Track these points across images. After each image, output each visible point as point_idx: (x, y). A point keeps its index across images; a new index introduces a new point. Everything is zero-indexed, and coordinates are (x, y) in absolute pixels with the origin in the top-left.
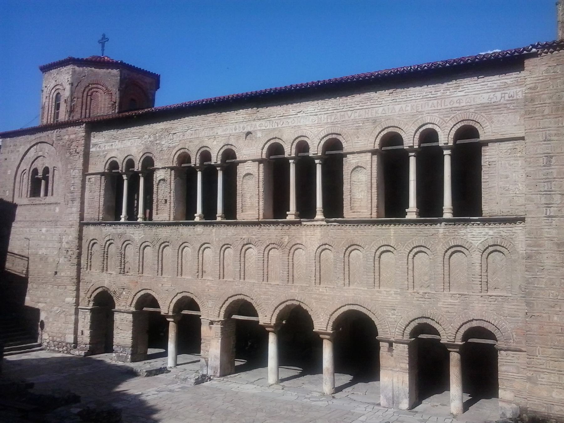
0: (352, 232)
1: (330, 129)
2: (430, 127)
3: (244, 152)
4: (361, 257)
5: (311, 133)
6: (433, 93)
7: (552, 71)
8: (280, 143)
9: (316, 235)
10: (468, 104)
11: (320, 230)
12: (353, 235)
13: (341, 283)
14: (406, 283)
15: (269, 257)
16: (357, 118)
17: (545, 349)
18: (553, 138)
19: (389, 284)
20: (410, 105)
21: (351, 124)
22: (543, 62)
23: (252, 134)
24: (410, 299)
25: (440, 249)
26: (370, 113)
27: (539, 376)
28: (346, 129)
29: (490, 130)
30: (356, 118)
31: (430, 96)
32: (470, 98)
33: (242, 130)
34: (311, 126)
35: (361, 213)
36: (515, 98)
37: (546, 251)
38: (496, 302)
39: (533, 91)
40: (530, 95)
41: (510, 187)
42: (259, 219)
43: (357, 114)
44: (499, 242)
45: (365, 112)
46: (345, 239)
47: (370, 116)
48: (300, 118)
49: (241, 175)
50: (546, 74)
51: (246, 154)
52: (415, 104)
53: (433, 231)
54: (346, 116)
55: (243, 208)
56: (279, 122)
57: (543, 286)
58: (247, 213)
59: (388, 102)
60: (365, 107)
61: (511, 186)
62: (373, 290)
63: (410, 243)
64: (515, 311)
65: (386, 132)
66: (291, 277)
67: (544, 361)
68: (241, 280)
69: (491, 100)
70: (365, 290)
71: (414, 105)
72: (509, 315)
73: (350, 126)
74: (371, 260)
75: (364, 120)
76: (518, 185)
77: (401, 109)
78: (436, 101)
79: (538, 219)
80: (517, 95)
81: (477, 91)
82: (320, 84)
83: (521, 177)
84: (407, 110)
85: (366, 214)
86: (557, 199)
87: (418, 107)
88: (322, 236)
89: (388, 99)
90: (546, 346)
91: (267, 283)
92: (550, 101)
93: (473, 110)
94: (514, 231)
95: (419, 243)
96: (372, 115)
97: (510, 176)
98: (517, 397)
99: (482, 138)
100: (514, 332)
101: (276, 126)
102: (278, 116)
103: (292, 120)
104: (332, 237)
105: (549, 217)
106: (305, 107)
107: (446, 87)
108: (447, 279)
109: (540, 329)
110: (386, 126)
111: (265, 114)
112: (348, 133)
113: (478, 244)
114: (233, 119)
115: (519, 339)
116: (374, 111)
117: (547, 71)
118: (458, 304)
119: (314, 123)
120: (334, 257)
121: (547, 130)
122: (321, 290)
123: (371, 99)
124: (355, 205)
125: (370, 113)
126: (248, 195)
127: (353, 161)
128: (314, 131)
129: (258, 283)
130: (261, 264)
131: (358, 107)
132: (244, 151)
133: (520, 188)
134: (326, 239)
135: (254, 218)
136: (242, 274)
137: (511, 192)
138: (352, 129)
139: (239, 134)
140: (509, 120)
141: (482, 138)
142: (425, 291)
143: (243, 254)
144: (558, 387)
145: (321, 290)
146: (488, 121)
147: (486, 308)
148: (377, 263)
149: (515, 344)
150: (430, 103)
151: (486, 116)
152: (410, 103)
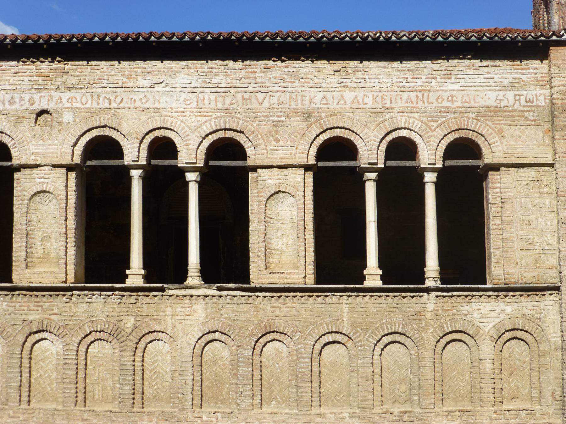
0: (268, 308)
1: (222, 121)
2: (405, 135)
3: (32, 148)
4: (285, 355)
5: (183, 125)
6: (409, 80)
8: (114, 137)
9: (196, 314)
10: (466, 104)
11: (204, 306)
12: (270, 314)
13: (245, 403)
14: (371, 397)
15: (89, 358)
16: (276, 106)
19: (337, 400)
20: (370, 95)
21: (263, 116)
23: (51, 114)
26: (299, 101)
28: (255, 125)
29: (500, 148)
30: (273, 106)
31: (404, 84)
32: (468, 95)
33: (27, 105)
34: (182, 112)
35: (285, 276)
36: (535, 104)
38: (518, 420)
40: (560, 102)
41: (535, 240)
42: (66, 282)
43: (275, 100)
44: (521, 324)
45: (290, 98)
46: (255, 322)
47: (300, 106)
48: (159, 94)
49: (26, 193)
51: (37, 153)
52: (380, 94)
53: (417, 307)
54: (253, 100)
55: (29, 260)
56: (113, 99)
58: (36, 270)
59: (332, 85)
60: (289, 89)
61: (536, 237)
62: (309, 412)
63: (377, 328)
65: (328, 136)
66: (138, 397)
68: (22, 406)
69: (500, 103)
70: (295, 414)
71: (377, 96)
73: (261, 118)
74: (306, 360)
75: (288, 111)
76: (547, 237)
77: (355, 100)
78: (413, 95)
80: (537, 99)
81: (479, 86)
82: (222, 38)
83: (549, 224)
84: (367, 103)
85: (295, 276)
87: (385, 99)
88: (207, 316)
89: (333, 80)
91: (83, 409)
93: (473, 115)
94: (542, 307)
95: (393, 328)
96: (302, 104)
97: (534, 222)
99: (488, 159)
101: (107, 105)
102: (110, 86)
103: (141, 95)
104: (229, 318)
106: (171, 76)
107: (430, 72)
108: (438, 388)
110: (328, 126)
111: (82, 80)
112: (258, 131)
113: (489, 328)
114: (7, 83)
116: (307, 98)
119: (189, 106)
120: (231, 354)
122: (205, 418)
123: (298, 76)
124: (271, 260)
125: (299, 101)
126: (38, 235)
127: (270, 181)
128: (190, 121)
129: (64, 410)
130: (71, 372)
131: (277, 88)
132: (31, 147)
133: (550, 241)
134: (217, 322)
135: (56, 280)
136: (25, 394)
137: (537, 247)
138: (265, 125)
139: (19, 112)
140: (528, 136)
141: (488, 159)
142: (403, 409)
143: (28, 352)
145: (205, 418)
148: (316, 364)
150: (405, 95)
151: (493, 126)
152: (371, 91)
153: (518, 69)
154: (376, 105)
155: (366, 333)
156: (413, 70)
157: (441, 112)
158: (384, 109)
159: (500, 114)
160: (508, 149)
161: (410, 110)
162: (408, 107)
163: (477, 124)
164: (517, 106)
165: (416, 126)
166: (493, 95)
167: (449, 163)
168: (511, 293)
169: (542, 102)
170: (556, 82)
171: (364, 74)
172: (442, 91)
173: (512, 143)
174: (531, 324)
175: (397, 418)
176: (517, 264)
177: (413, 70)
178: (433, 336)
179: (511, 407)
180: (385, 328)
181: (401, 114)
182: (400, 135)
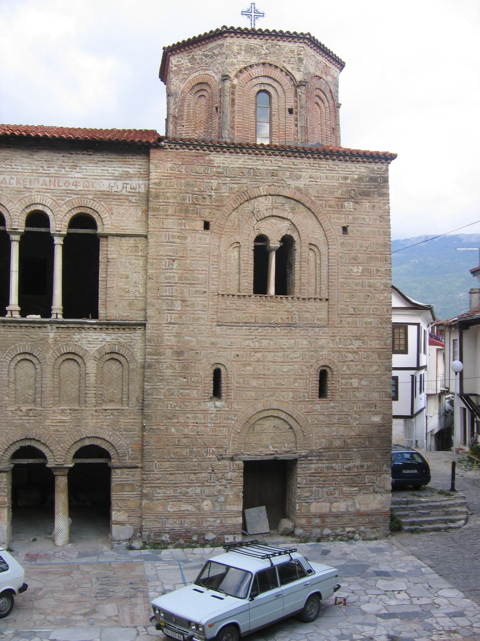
2: (40, 209)
6: (45, 168)
7: (177, 170)
10: (86, 189)
17: (161, 463)
18: (176, 240)
20: (15, 177)
22: (169, 158)
24: (10, 419)
25: (50, 355)
27: (156, 491)
29: (109, 222)
36: (137, 191)
37: (165, 360)
39: (158, 187)
40: (154, 190)
41: (130, 289)
44: (117, 349)
50: (171, 172)
57: (162, 397)
61: (131, 288)
63: (12, 349)
64: (132, 425)
67: (161, 476)
69: (111, 189)
72: (125, 430)
76: (139, 287)
77: (4, 181)
78: (47, 179)
79: (158, 325)
80: (139, 188)
86: (178, 306)
87: (26, 182)
90: (163, 460)
92: (174, 201)
93: (91, 197)
94: (133, 338)
97: (130, 277)
98: (131, 516)
100: (131, 447)
105: (170, 323)
109: (158, 442)
113: (93, 351)
115: (134, 454)
117: (171, 169)
118: (70, 421)
121: (170, 231)
140: (130, 214)
141: (99, 231)
142: (30, 408)
144: (173, 500)
146: (107, 211)
147: (101, 424)
149: (130, 461)
150: (41, 180)
152: (16, 175)
153: (127, 164)
154: (19, 186)
155: (4, 353)
156: (49, 161)
157: (67, 193)
158: (25, 189)
159: (111, 197)
160: (115, 222)
161: (44, 190)
162: (43, 189)
163: (93, 203)
164: (124, 192)
165: (48, 203)
166: (106, 183)
167: (73, 231)
168: (111, 327)
169: (143, 190)
170: (153, 175)
171: (11, 162)
172: (69, 177)
173: (118, 218)
174: (124, 350)
175: (25, 414)
176: (116, 306)
177: (49, 161)
178: (53, 356)
179: (107, 408)
180: (18, 349)
181: (38, 193)
182: (36, 209)
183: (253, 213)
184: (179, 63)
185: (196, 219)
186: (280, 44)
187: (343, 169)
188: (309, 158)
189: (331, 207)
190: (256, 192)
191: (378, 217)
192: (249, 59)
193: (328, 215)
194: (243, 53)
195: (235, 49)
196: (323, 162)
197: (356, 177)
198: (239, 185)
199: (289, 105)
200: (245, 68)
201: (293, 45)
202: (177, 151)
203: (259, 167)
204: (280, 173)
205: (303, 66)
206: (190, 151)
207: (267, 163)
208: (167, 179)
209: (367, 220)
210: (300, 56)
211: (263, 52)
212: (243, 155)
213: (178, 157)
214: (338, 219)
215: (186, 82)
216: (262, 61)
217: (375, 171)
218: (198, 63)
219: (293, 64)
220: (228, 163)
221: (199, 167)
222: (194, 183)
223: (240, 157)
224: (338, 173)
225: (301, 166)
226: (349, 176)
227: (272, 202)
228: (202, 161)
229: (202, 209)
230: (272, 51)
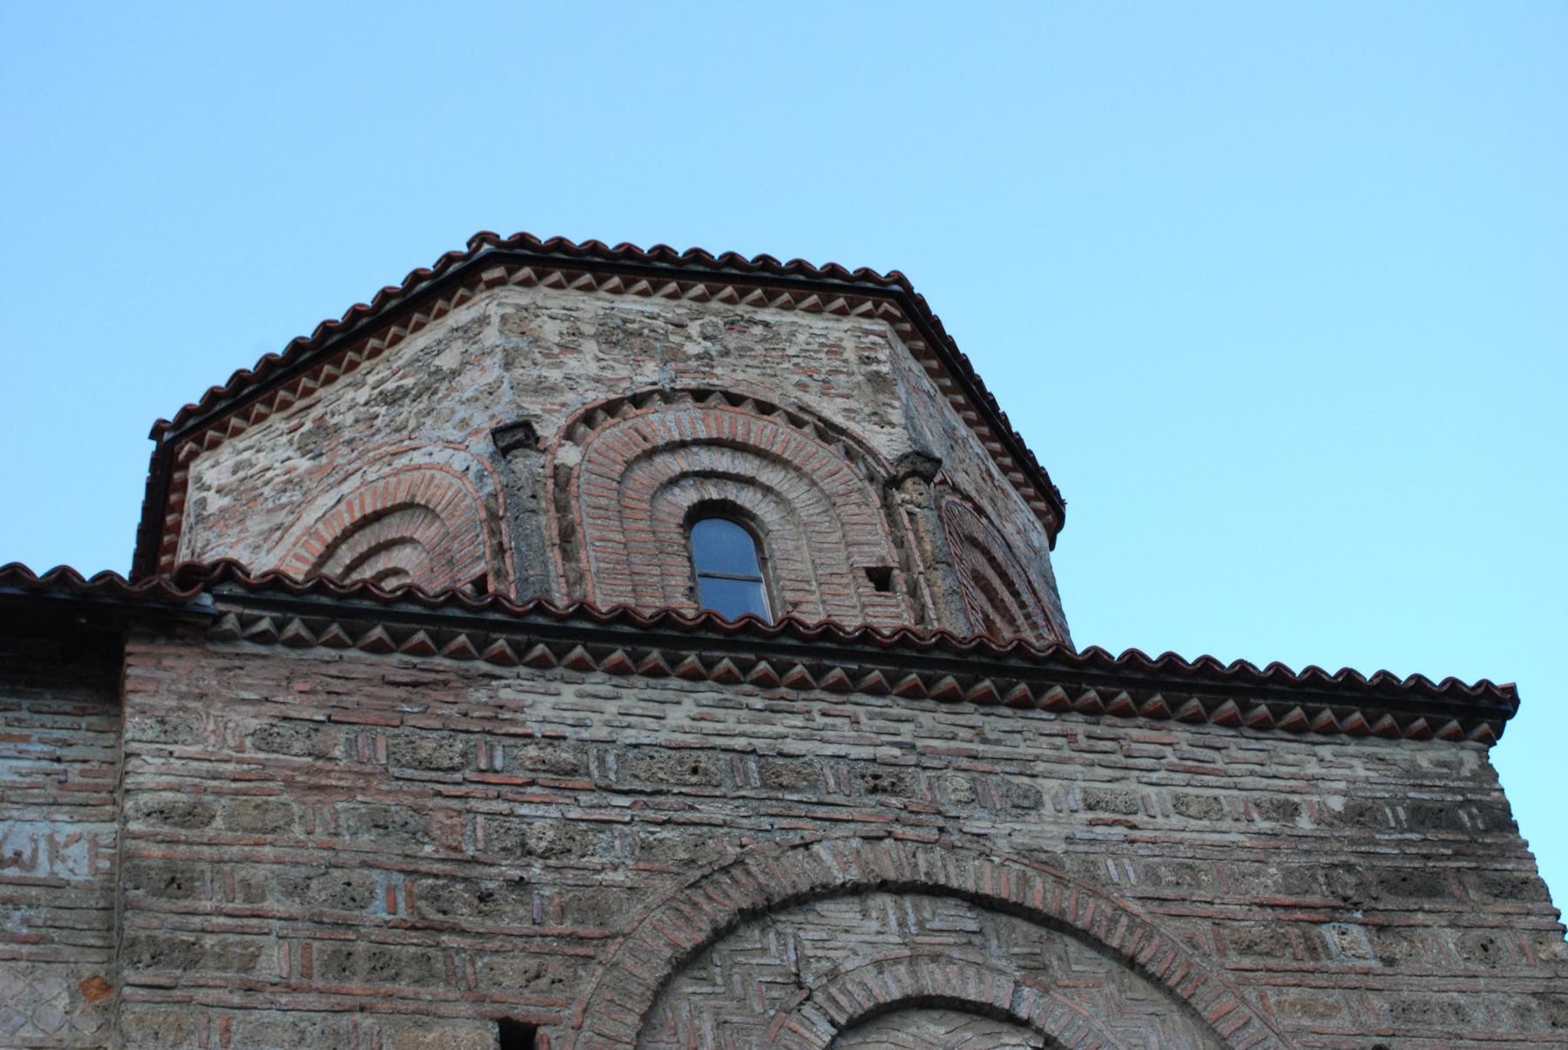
22: (247, 687)
36: (42, 871)
39: (183, 833)
40: (157, 851)
50: (262, 755)
80: (55, 854)
92: (294, 907)
117: (265, 739)
169: (78, 865)
183: (800, 985)
184: (241, 474)
185: (444, 1009)
186: (769, 318)
187: (1258, 768)
188: (1058, 708)
189: (1248, 949)
190: (796, 873)
191: (1534, 1004)
192: (623, 371)
193: (1251, 995)
194: (590, 347)
195: (551, 331)
196: (1136, 733)
197: (1337, 803)
198: (691, 829)
199: (872, 555)
200: (612, 408)
201: (830, 324)
202: (294, 654)
203: (791, 746)
204: (920, 783)
205: (897, 404)
206: (374, 658)
207: (834, 727)
208: (237, 793)
209: (1479, 1016)
210: (874, 367)
211: (692, 349)
212: (686, 684)
213: (299, 685)
214: (1307, 1010)
215: (289, 539)
216: (693, 384)
217: (1425, 776)
218: (350, 442)
219: (848, 397)
220: (608, 724)
221: (434, 735)
222: (415, 822)
223: (670, 695)
224: (1236, 787)
225: (1024, 749)
226: (1296, 798)
227: (902, 924)
228: (452, 711)
229: (481, 952)
230: (731, 346)
